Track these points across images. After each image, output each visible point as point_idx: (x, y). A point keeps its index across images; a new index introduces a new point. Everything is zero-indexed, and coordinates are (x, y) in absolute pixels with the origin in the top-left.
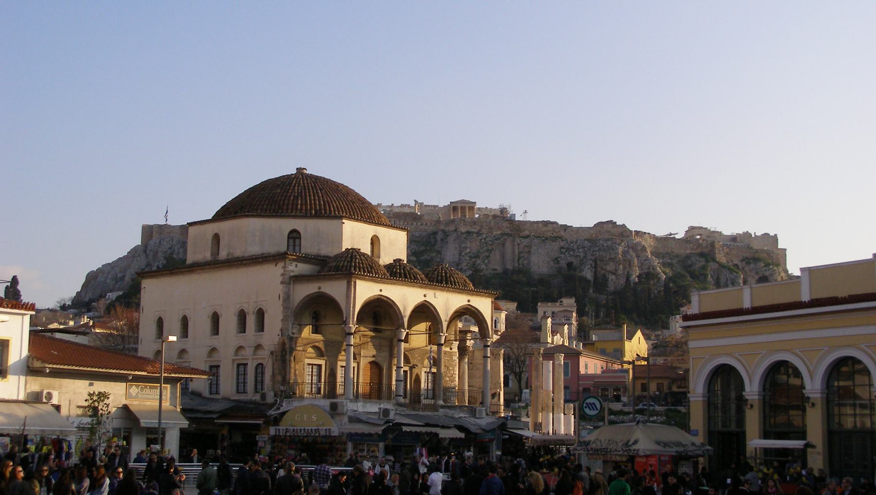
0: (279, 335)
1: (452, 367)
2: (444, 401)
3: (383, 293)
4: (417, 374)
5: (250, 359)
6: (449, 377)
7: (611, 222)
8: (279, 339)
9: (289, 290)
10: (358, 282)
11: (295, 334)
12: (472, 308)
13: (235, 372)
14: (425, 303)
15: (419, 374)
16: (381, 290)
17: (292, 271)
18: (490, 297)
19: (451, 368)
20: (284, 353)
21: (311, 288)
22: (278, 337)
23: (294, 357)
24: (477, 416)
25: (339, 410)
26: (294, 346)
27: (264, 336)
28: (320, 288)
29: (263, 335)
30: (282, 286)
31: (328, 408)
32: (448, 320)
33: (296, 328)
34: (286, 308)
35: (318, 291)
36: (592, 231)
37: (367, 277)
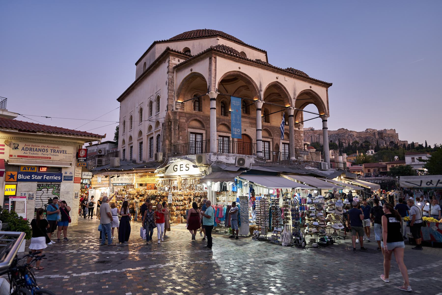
0: (166, 111)
1: (300, 140)
2: (297, 157)
4: (277, 143)
5: (154, 133)
6: (299, 147)
7: (343, 129)
8: (166, 113)
9: (172, 77)
10: (218, 58)
11: (179, 109)
12: (313, 93)
13: (149, 144)
14: (277, 83)
16: (239, 68)
17: (175, 64)
18: (325, 87)
19: (300, 141)
20: (170, 123)
21: (186, 73)
24: (323, 169)
26: (178, 118)
27: (159, 114)
28: (191, 70)
29: (159, 114)
30: (168, 74)
32: (296, 98)
33: (179, 105)
35: (190, 72)
36: (337, 132)
37: (226, 55)
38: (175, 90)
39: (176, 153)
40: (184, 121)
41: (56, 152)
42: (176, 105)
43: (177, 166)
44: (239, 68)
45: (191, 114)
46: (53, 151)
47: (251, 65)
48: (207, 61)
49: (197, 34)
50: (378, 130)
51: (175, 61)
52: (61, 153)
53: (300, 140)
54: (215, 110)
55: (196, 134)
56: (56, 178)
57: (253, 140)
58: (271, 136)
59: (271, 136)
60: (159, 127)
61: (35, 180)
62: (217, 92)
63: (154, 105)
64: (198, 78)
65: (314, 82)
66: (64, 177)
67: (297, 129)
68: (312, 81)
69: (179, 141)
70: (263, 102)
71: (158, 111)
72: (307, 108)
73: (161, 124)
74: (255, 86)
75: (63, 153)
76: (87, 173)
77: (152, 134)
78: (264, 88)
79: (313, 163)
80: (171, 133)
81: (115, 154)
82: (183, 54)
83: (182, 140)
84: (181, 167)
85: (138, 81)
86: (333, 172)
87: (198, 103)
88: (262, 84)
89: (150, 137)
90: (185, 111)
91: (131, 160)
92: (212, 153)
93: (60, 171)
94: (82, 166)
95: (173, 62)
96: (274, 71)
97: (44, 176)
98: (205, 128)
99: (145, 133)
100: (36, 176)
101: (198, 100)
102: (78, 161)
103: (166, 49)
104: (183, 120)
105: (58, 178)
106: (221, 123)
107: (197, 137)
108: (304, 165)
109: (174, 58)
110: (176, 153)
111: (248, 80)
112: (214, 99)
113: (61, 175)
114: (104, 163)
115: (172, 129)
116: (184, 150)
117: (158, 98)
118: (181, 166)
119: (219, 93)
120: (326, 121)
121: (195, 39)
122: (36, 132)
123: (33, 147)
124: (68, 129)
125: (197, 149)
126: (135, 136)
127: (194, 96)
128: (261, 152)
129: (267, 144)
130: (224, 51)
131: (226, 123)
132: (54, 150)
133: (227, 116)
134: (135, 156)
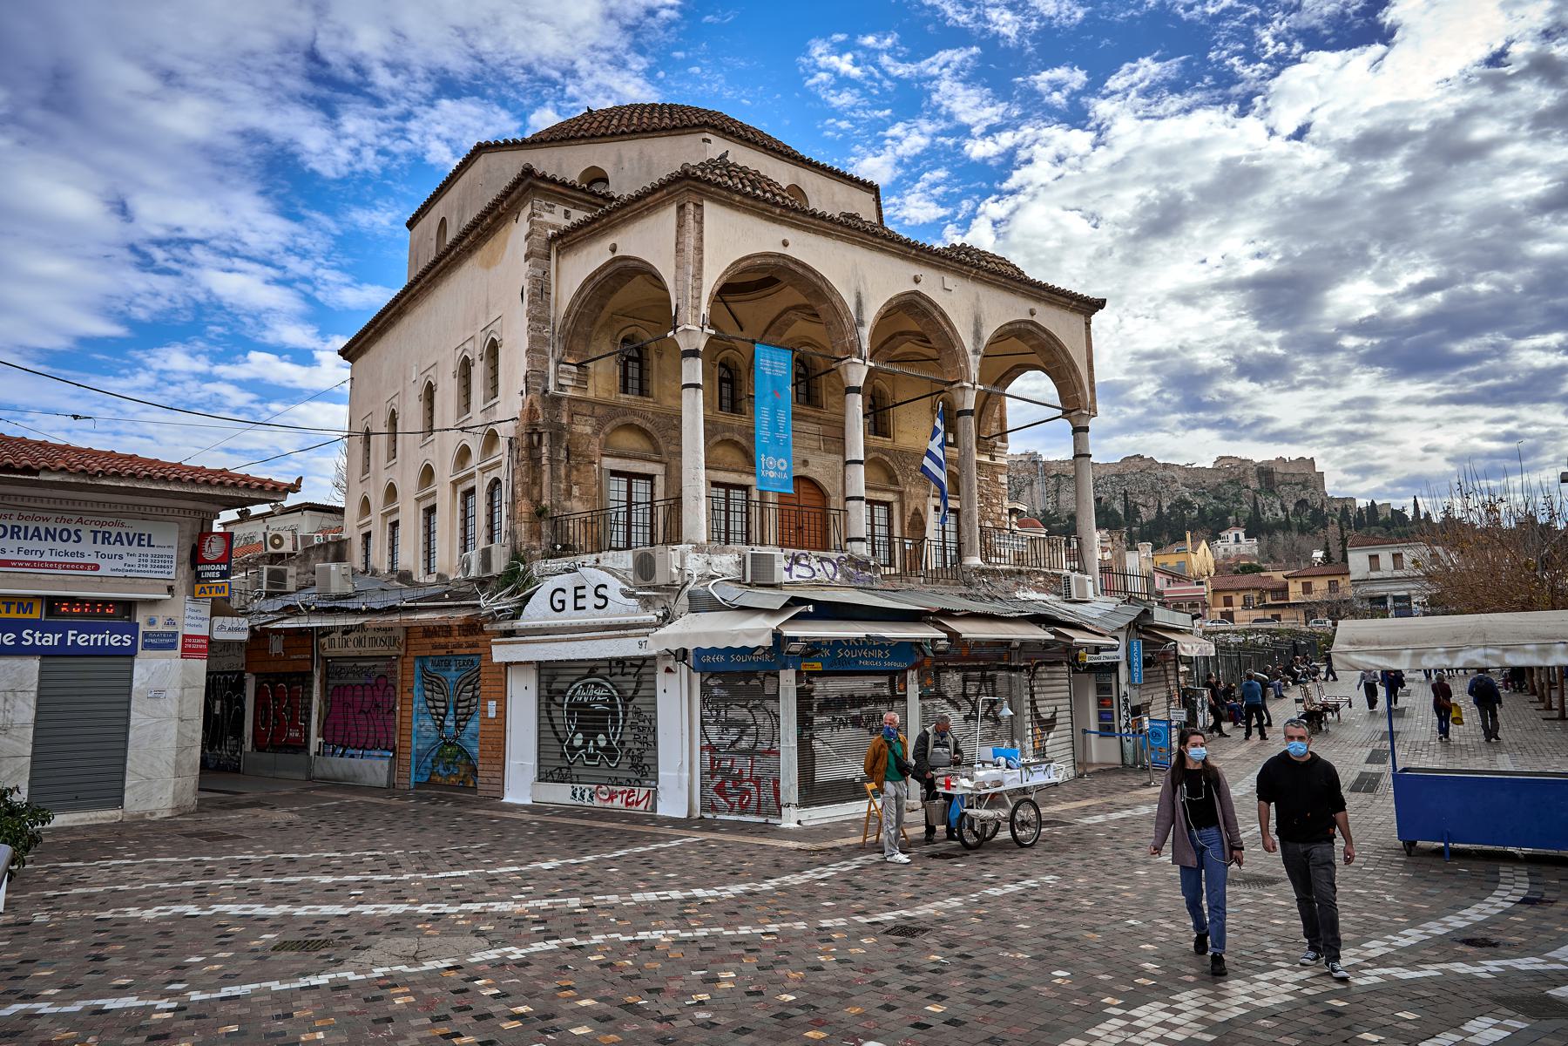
2: (985, 559)
3: (788, 252)
4: (916, 509)
10: (708, 206)
13: (458, 515)
14: (918, 298)
15: (921, 509)
16: (785, 244)
17: (553, 227)
18: (1081, 312)
20: (535, 438)
22: (520, 398)
23: (567, 449)
24: (1074, 597)
25: (660, 579)
26: (565, 421)
31: (631, 575)
33: (570, 373)
34: (538, 319)
35: (609, 256)
37: (738, 198)
38: (555, 319)
39: (559, 547)
40: (588, 430)
41: (112, 540)
42: (557, 371)
43: (564, 591)
44: (785, 244)
45: (613, 409)
46: (100, 536)
47: (826, 234)
48: (669, 215)
49: (630, 119)
50: (1257, 460)
51: (557, 217)
52: (130, 544)
53: (996, 495)
54: (701, 392)
55: (630, 476)
56: (113, 640)
57: (834, 498)
58: (897, 484)
59: (897, 484)
60: (496, 452)
61: (32, 651)
62: (706, 329)
63: (478, 372)
64: (638, 278)
65: (1044, 293)
66: (146, 635)
67: (986, 459)
68: (1035, 290)
69: (568, 504)
70: (868, 363)
71: (491, 393)
72: (1019, 385)
73: (502, 446)
74: (839, 305)
75: (139, 545)
76: (229, 621)
77: (472, 476)
78: (871, 314)
79: (1041, 579)
80: (541, 473)
81: (332, 549)
82: (583, 190)
83: (580, 499)
84: (576, 597)
85: (417, 287)
86: (1112, 607)
87: (636, 365)
88: (864, 300)
89: (461, 488)
90: (591, 394)
91: (392, 571)
92: (690, 546)
93: (129, 614)
94: (214, 595)
95: (547, 217)
96: (904, 256)
97: (70, 632)
98: (664, 454)
99: (445, 474)
100: (38, 635)
101: (636, 355)
102: (198, 577)
103: (523, 172)
104: (584, 428)
105: (121, 641)
106: (719, 438)
107: (634, 490)
108: (1010, 583)
109: (549, 206)
110: (559, 547)
111: (815, 284)
112: (694, 353)
113: (133, 629)
114: (291, 584)
115: (544, 461)
116: (589, 534)
117: (493, 349)
118: (580, 592)
119: (713, 332)
120: (1086, 429)
121: (625, 137)
122: (36, 473)
123: (22, 524)
124: (157, 460)
125: (634, 529)
126: (408, 486)
127: (624, 341)
128: (863, 540)
129: (881, 512)
130: (730, 183)
131: (737, 438)
132: (104, 533)
133: (741, 412)
134: (409, 557)
